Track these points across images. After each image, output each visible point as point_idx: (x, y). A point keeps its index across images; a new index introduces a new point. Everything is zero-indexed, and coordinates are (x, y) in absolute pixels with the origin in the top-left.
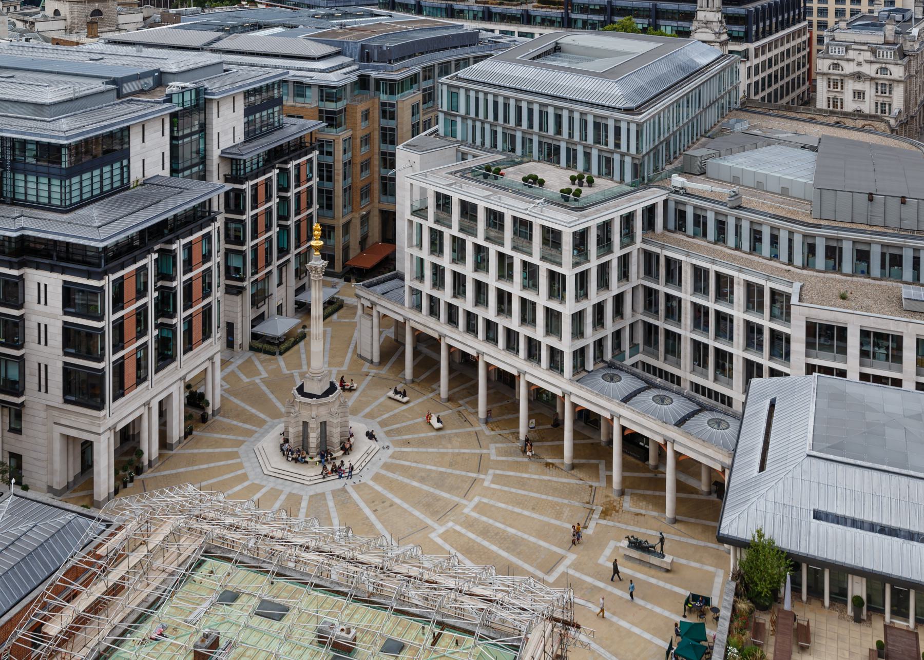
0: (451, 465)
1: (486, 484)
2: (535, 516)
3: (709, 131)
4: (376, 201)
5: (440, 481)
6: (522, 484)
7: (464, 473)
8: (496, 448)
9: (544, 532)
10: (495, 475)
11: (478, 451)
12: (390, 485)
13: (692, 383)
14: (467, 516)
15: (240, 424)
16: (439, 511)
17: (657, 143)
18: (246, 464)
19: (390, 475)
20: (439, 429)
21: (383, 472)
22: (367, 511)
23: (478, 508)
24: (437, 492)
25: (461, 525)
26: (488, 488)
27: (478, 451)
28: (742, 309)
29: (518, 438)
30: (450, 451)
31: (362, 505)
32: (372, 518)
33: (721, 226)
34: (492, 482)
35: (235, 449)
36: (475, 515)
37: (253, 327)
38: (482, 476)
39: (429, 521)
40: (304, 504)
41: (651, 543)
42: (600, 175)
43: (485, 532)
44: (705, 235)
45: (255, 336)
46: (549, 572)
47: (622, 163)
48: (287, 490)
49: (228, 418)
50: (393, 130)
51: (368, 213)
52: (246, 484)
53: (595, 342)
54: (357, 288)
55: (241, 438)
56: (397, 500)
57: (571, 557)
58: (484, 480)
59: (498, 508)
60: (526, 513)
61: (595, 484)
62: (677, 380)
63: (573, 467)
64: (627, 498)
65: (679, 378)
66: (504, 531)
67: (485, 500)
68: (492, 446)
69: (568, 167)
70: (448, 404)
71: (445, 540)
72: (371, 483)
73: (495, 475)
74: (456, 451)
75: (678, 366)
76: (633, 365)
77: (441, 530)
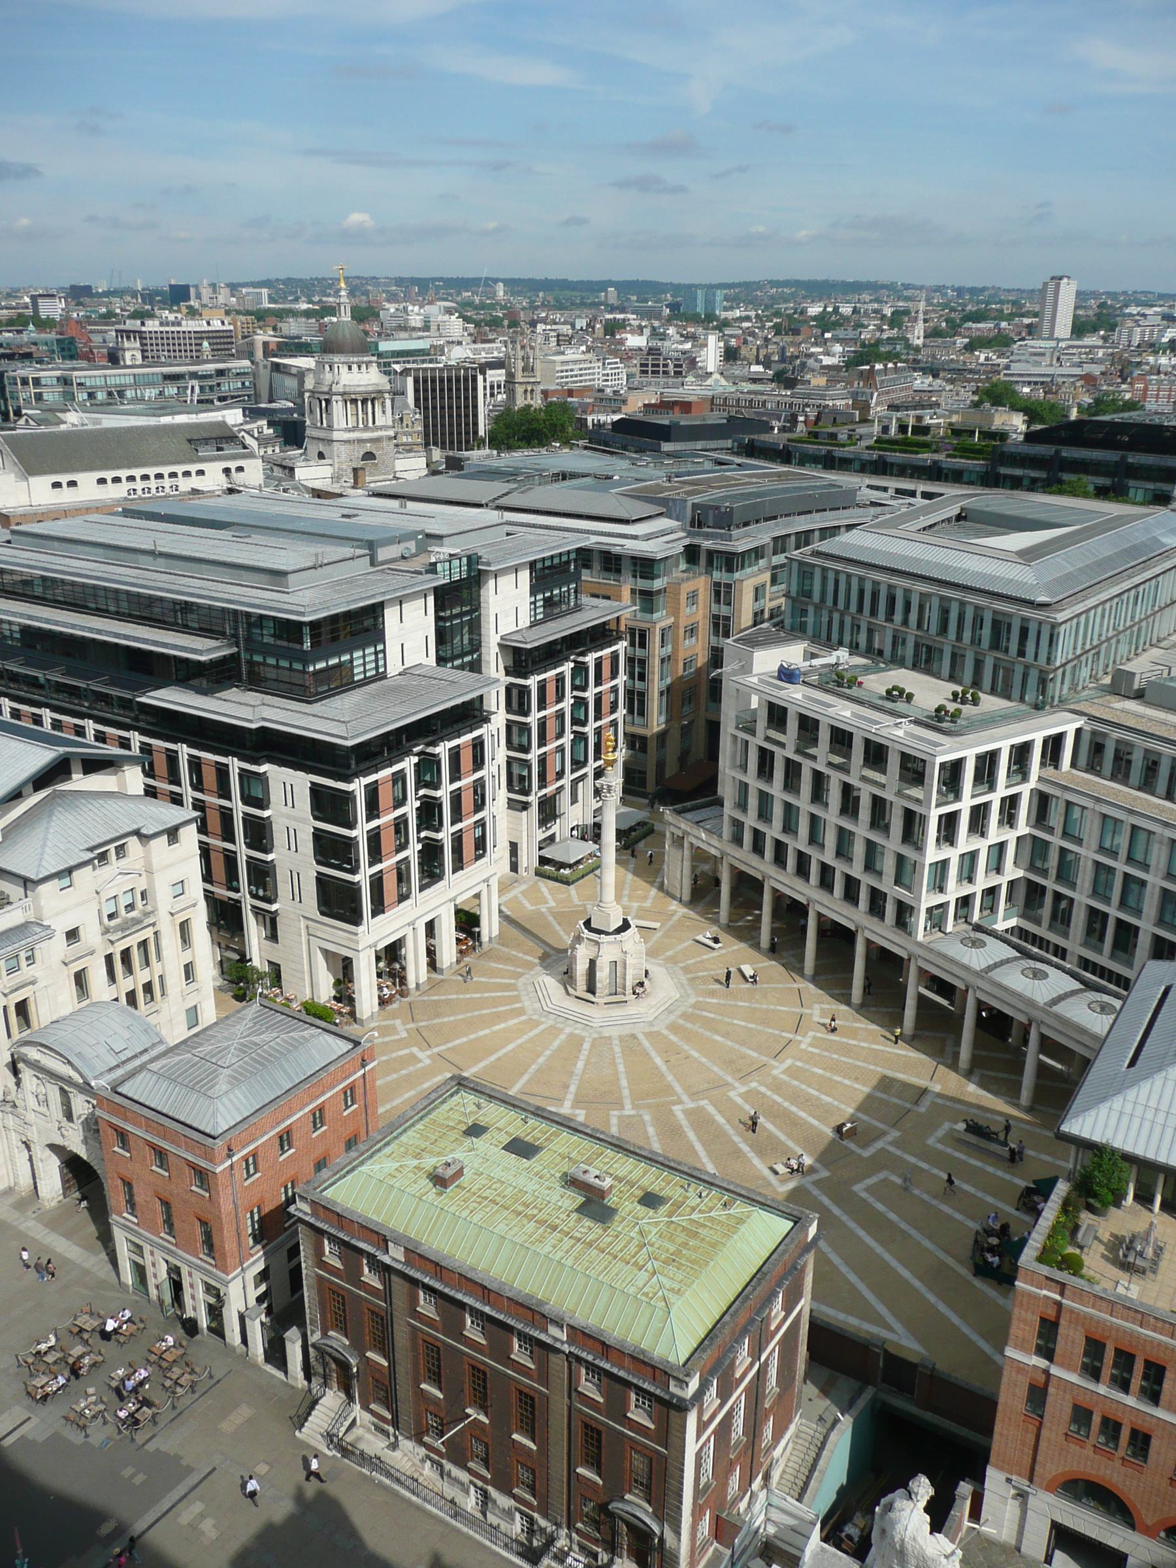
1: (803, 1046)
3: (1164, 639)
4: (703, 708)
8: (822, 1009)
11: (799, 1010)
12: (688, 1036)
13: (1080, 957)
14: (775, 1078)
15: (521, 955)
17: (1079, 652)
18: (523, 998)
19: (689, 1025)
21: (681, 1022)
22: (658, 1061)
24: (743, 1050)
25: (767, 1087)
26: (805, 1051)
27: (799, 1010)
28: (1160, 874)
31: (653, 1054)
32: (664, 1068)
33: (1152, 767)
34: (811, 1045)
35: (512, 981)
36: (783, 1077)
37: (540, 849)
38: (799, 1038)
40: (586, 1046)
41: (993, 1129)
42: (993, 691)
43: (795, 1097)
44: (1127, 776)
45: (543, 861)
47: (1025, 676)
48: (568, 1030)
49: (508, 947)
50: (727, 619)
51: (691, 723)
52: (523, 1018)
53: (957, 899)
54: (667, 812)
55: (520, 970)
56: (695, 1054)
57: (895, 1134)
58: (800, 1042)
59: (814, 1074)
60: (847, 1082)
62: (1061, 952)
65: (1064, 951)
66: (818, 1098)
67: (799, 1064)
68: (817, 1006)
69: (952, 678)
71: (746, 1101)
72: (665, 1032)
73: (814, 1038)
74: (772, 1007)
75: (1065, 935)
76: (1007, 931)
77: (743, 1089)
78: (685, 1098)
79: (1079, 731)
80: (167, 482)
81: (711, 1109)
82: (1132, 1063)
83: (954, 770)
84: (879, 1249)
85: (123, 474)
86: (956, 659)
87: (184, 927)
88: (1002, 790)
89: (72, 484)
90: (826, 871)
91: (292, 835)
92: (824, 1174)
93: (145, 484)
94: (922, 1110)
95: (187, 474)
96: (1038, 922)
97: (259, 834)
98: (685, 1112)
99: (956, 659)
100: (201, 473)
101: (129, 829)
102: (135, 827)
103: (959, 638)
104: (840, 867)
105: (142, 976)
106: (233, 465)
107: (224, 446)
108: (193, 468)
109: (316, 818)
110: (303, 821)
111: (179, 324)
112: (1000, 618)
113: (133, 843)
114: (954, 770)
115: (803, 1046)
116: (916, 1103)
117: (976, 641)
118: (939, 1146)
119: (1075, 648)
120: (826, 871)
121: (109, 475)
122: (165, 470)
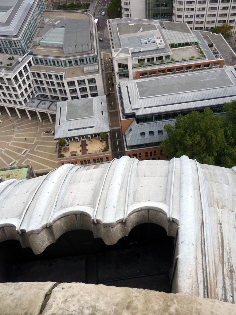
0: (8, 129)
1: (16, 130)
2: (27, 133)
5: (6, 133)
6: (22, 127)
7: (11, 130)
9: (30, 136)
10: (17, 128)
14: (15, 138)
16: (8, 140)
20: (2, 122)
23: (16, 136)
24: (7, 136)
26: (17, 131)
29: (19, 118)
30: (6, 126)
34: (17, 129)
39: (7, 142)
43: (19, 140)
46: (33, 143)
59: (20, 134)
61: (37, 122)
63: (32, 119)
64: (44, 122)
67: (17, 134)
68: (15, 122)
70: (2, 115)
74: (7, 126)
77: (11, 143)
78: (2, 149)
79: (32, 58)
81: (7, 149)
82: (60, 124)
83: (16, 78)
84: (42, 158)
86: (6, 50)
88: (25, 75)
90: (4, 100)
92: (29, 150)
94: (38, 132)
96: (41, 92)
98: (4, 152)
99: (6, 50)
103: (4, 45)
104: (6, 99)
112: (9, 41)
114: (16, 78)
115: (16, 130)
116: (37, 131)
117: (7, 45)
118: (43, 137)
119: (24, 40)
120: (4, 100)
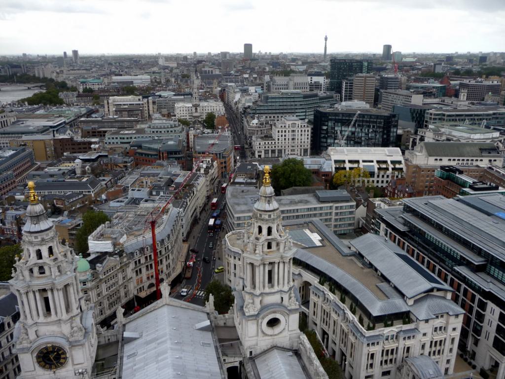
80: (470, 162)
85: (457, 158)
87: (453, 340)
89: (441, 160)
91: (490, 323)
93: (463, 162)
95: (477, 160)
97: (480, 317)
100: (481, 160)
101: (445, 312)
102: (447, 311)
105: (438, 348)
106: (493, 159)
107: (491, 151)
108: (479, 159)
109: (499, 321)
110: (495, 320)
111: (482, 82)
113: (445, 316)
121: (452, 158)
122: (470, 159)
